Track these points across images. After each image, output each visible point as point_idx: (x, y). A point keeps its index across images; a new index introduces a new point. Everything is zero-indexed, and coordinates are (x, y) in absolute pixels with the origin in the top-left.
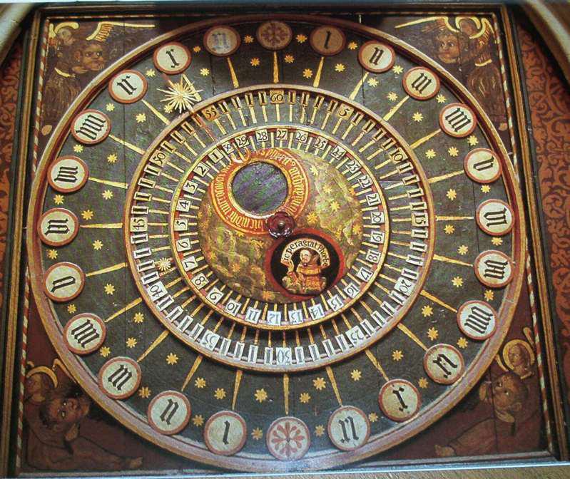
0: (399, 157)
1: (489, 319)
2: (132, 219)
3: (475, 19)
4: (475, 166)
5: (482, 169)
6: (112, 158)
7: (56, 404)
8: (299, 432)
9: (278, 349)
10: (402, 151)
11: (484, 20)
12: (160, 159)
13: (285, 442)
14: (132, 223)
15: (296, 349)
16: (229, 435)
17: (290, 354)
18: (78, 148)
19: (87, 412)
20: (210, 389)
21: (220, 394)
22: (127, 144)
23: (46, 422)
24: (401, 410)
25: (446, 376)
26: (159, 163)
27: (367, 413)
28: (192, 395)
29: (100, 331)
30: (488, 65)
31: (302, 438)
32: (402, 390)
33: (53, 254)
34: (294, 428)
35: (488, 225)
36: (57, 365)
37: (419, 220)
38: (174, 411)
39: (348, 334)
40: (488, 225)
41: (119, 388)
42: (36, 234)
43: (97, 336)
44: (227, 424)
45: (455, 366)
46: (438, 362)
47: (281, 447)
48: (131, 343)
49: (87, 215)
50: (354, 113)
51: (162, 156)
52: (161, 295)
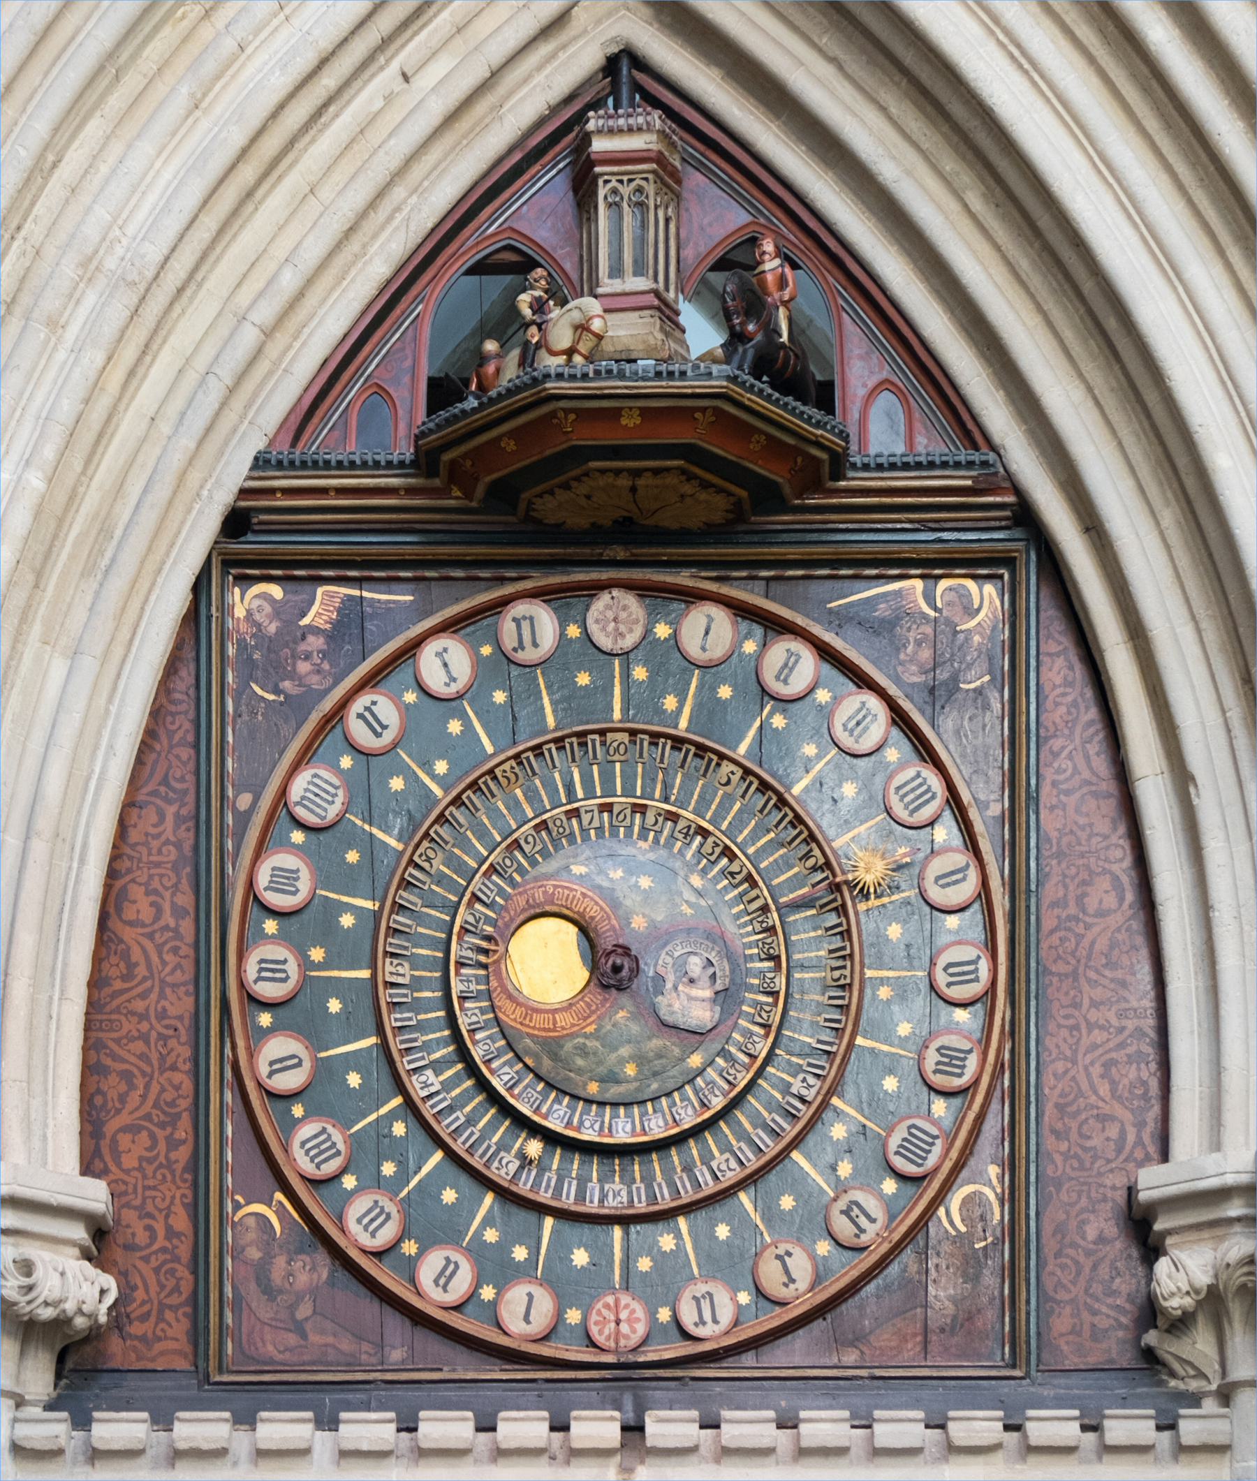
0: (811, 862)
1: (932, 1144)
2: (388, 960)
3: (971, 584)
4: (938, 879)
5: (948, 885)
6: (352, 857)
7: (280, 1262)
8: (633, 1311)
9: (607, 1187)
10: (817, 852)
11: (989, 589)
12: (428, 860)
13: (613, 1325)
14: (388, 968)
15: (634, 1187)
16: (533, 1311)
17: (624, 1193)
18: (298, 837)
19: (325, 1275)
20: (503, 1247)
21: (520, 1253)
22: (375, 831)
23: (269, 1291)
24: (786, 1285)
25: (857, 1236)
26: (426, 865)
27: (735, 1290)
28: (477, 1252)
29: (341, 1146)
30: (982, 686)
31: (638, 1320)
32: (789, 1254)
33: (265, 1019)
34: (627, 1306)
35: (949, 985)
36: (280, 1203)
37: (837, 974)
38: (453, 1273)
39: (714, 1164)
40: (949, 985)
41: (373, 1235)
42: (242, 985)
43: (338, 1153)
44: (530, 1296)
45: (873, 1221)
46: (846, 1213)
47: (606, 1332)
48: (388, 1169)
49: (317, 954)
50: (743, 778)
51: (431, 854)
52: (433, 1089)
